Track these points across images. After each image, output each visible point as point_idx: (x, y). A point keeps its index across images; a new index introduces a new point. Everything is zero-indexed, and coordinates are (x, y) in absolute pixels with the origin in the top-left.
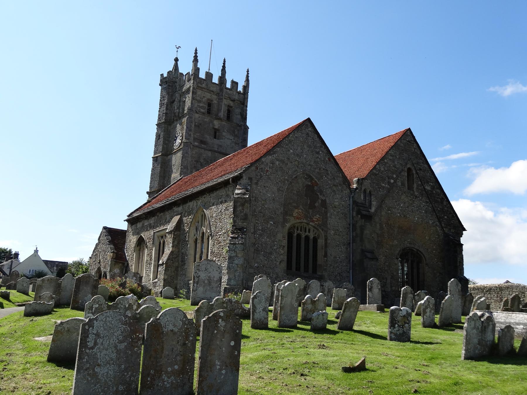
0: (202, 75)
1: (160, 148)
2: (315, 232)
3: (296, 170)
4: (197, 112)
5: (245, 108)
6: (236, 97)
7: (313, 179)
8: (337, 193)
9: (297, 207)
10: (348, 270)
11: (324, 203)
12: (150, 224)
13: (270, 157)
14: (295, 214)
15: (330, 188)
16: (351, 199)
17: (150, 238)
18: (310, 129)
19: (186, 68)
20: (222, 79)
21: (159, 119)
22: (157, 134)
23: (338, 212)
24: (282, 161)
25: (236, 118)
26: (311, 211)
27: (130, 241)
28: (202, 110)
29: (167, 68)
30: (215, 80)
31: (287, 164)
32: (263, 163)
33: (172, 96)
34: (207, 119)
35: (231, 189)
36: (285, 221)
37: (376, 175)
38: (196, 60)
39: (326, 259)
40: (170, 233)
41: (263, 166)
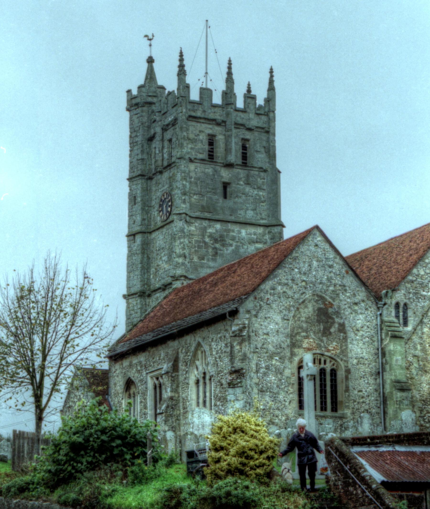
0: (195, 96)
1: (139, 218)
2: (332, 363)
3: (304, 293)
4: (191, 161)
5: (271, 137)
6: (255, 122)
7: (326, 300)
8: (359, 311)
9: (307, 337)
10: (378, 405)
11: (342, 328)
12: (140, 362)
13: (270, 282)
14: (305, 345)
15: (349, 307)
16: (379, 318)
17: (141, 381)
18: (319, 239)
19: (168, 80)
20: (229, 94)
21: (132, 168)
22: (130, 195)
23: (362, 336)
24: (287, 284)
25: (259, 158)
26: (325, 339)
27: (115, 384)
28: (200, 156)
29: (136, 79)
30: (217, 99)
31: (291, 288)
32: (262, 290)
33: (149, 127)
34: (209, 170)
35: (229, 323)
36: (293, 354)
37: (412, 282)
38: (182, 71)
39: (347, 394)
40: (167, 373)
41: (262, 294)
